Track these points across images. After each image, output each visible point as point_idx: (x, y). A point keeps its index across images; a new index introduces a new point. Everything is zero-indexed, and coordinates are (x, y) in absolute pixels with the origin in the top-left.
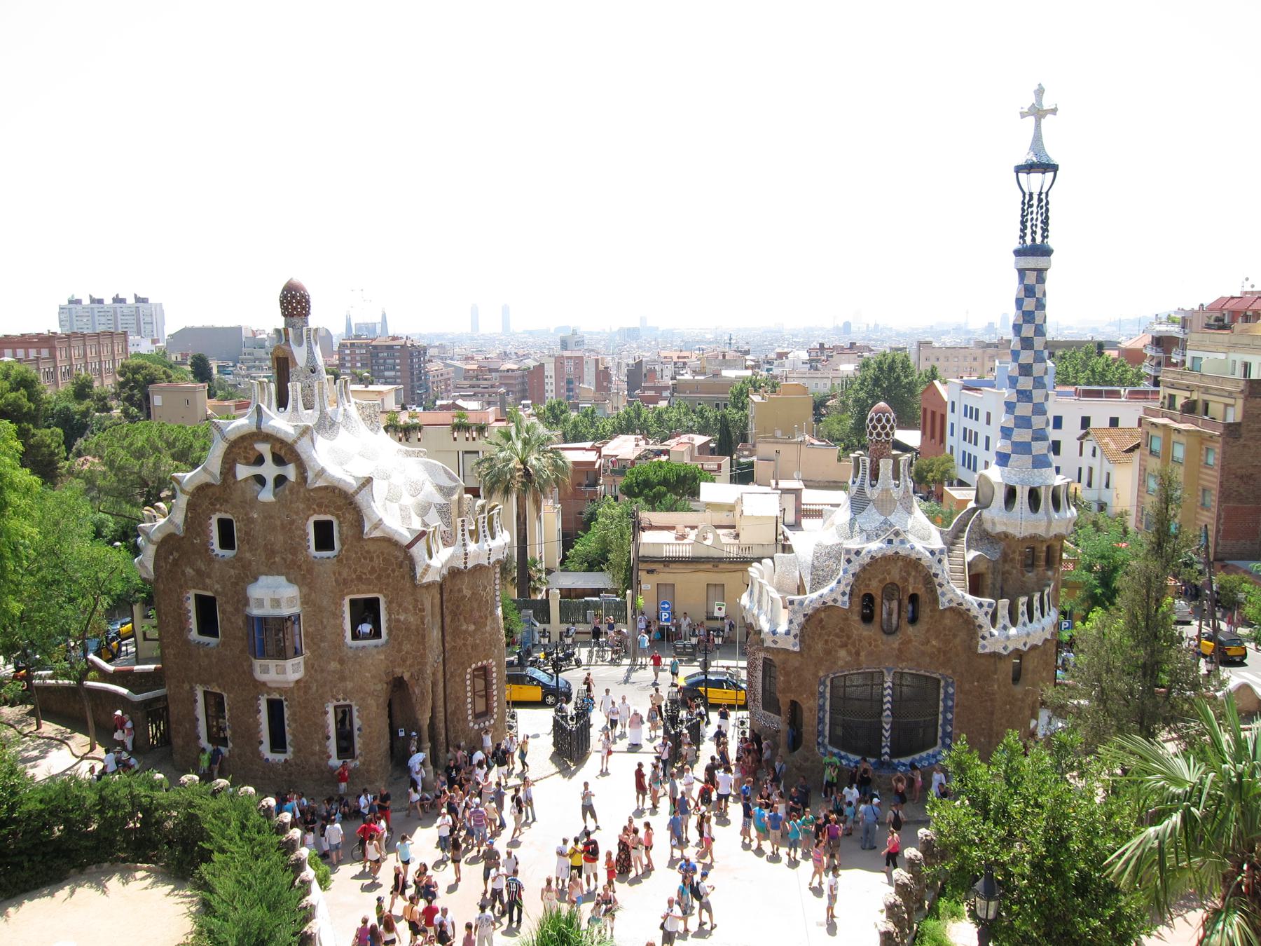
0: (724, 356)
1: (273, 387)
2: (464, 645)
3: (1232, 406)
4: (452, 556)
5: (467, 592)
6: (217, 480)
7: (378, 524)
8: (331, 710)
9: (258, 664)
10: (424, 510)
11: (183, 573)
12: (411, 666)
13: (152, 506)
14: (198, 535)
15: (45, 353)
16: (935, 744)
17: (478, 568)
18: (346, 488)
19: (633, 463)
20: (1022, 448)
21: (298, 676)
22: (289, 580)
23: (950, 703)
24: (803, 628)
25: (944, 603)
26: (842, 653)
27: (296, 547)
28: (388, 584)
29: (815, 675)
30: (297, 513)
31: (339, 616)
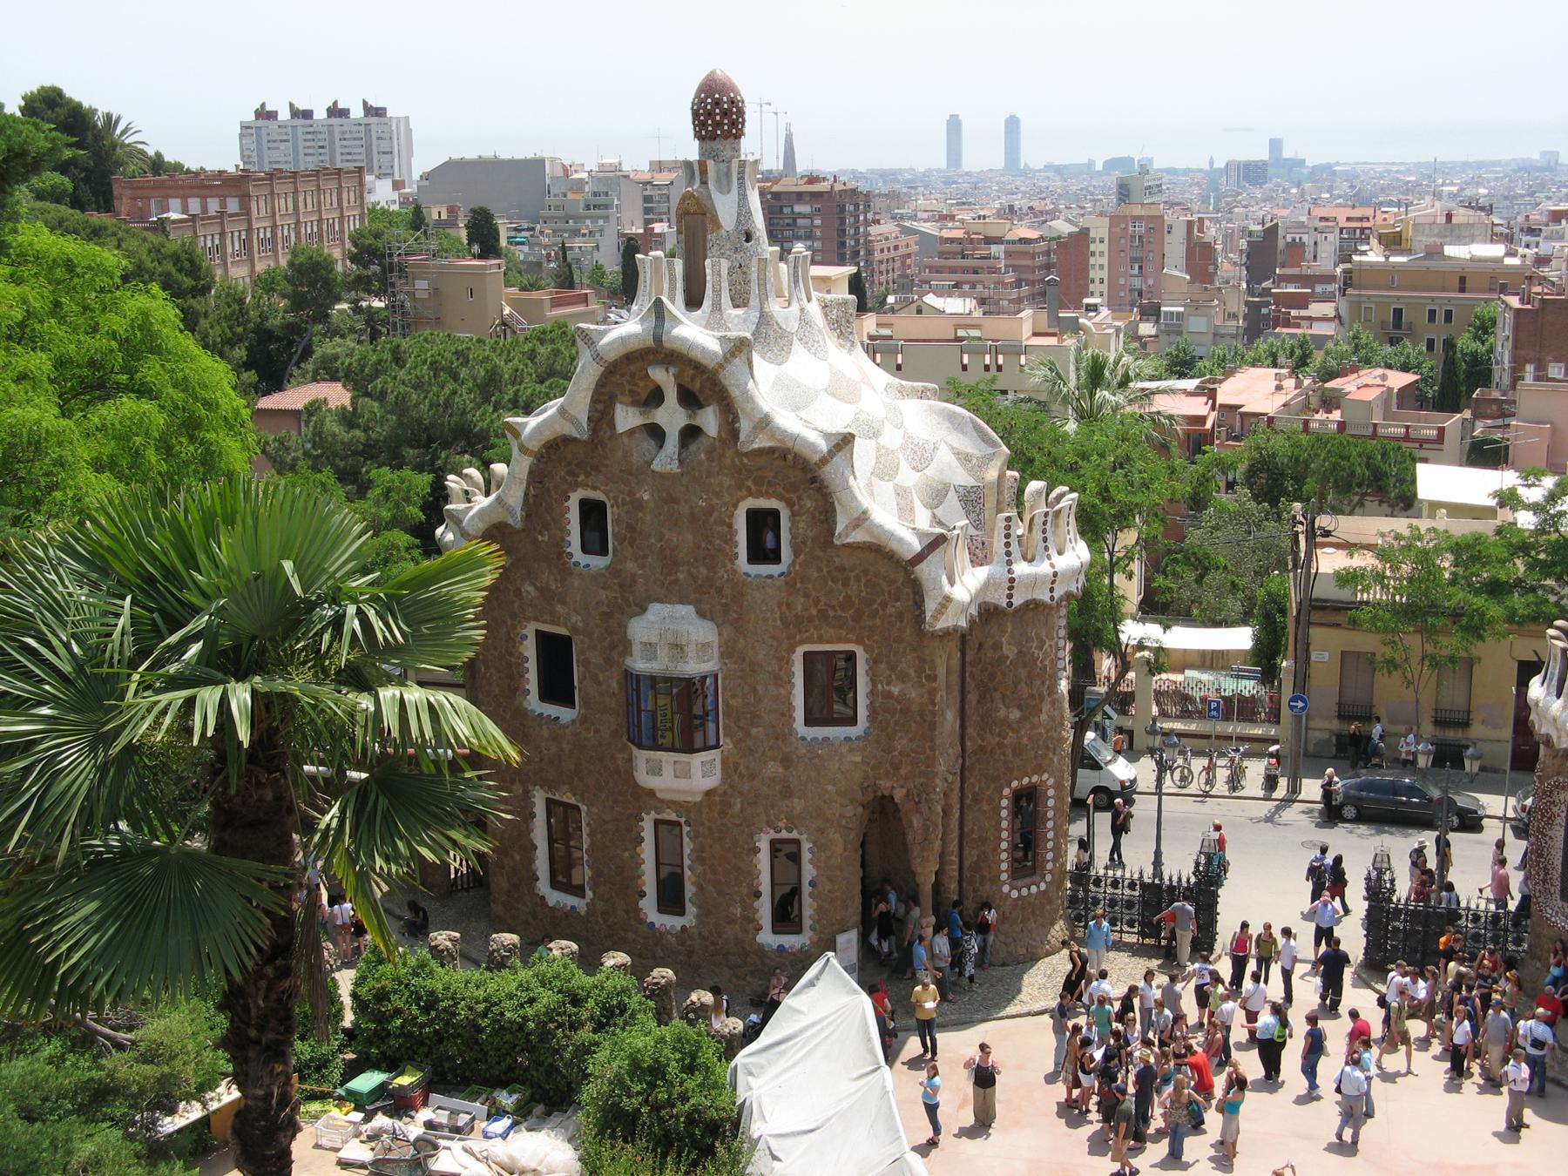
0: (1449, 217)
1: (679, 264)
2: (1000, 745)
4: (987, 586)
5: (1009, 651)
6: (581, 431)
7: (862, 519)
8: (764, 845)
9: (642, 757)
10: (936, 496)
11: (518, 593)
12: (907, 778)
13: (460, 475)
15: (233, 205)
17: (1033, 606)
18: (806, 453)
19: (1271, 420)
21: (712, 782)
22: (701, 614)
30: (718, 495)
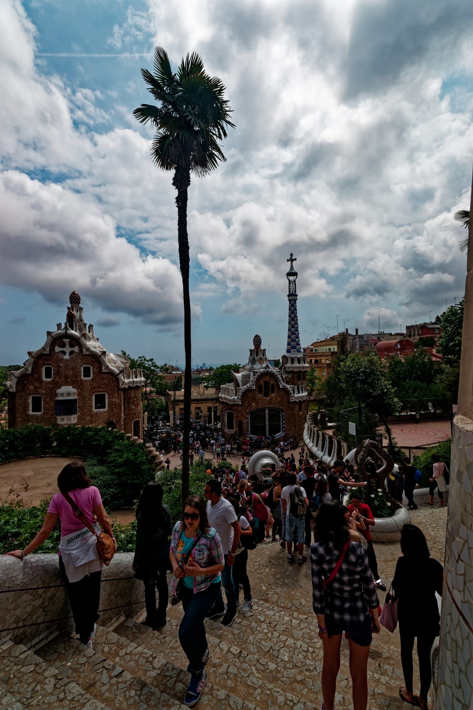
2: (132, 413)
3: (328, 359)
5: (133, 395)
9: (59, 418)
11: (28, 389)
14: (37, 373)
16: (280, 431)
20: (293, 348)
22: (73, 387)
23: (284, 418)
24: (242, 396)
25: (281, 387)
26: (254, 404)
27: (77, 375)
28: (109, 389)
29: (246, 411)
30: (78, 364)
31: (90, 400)
